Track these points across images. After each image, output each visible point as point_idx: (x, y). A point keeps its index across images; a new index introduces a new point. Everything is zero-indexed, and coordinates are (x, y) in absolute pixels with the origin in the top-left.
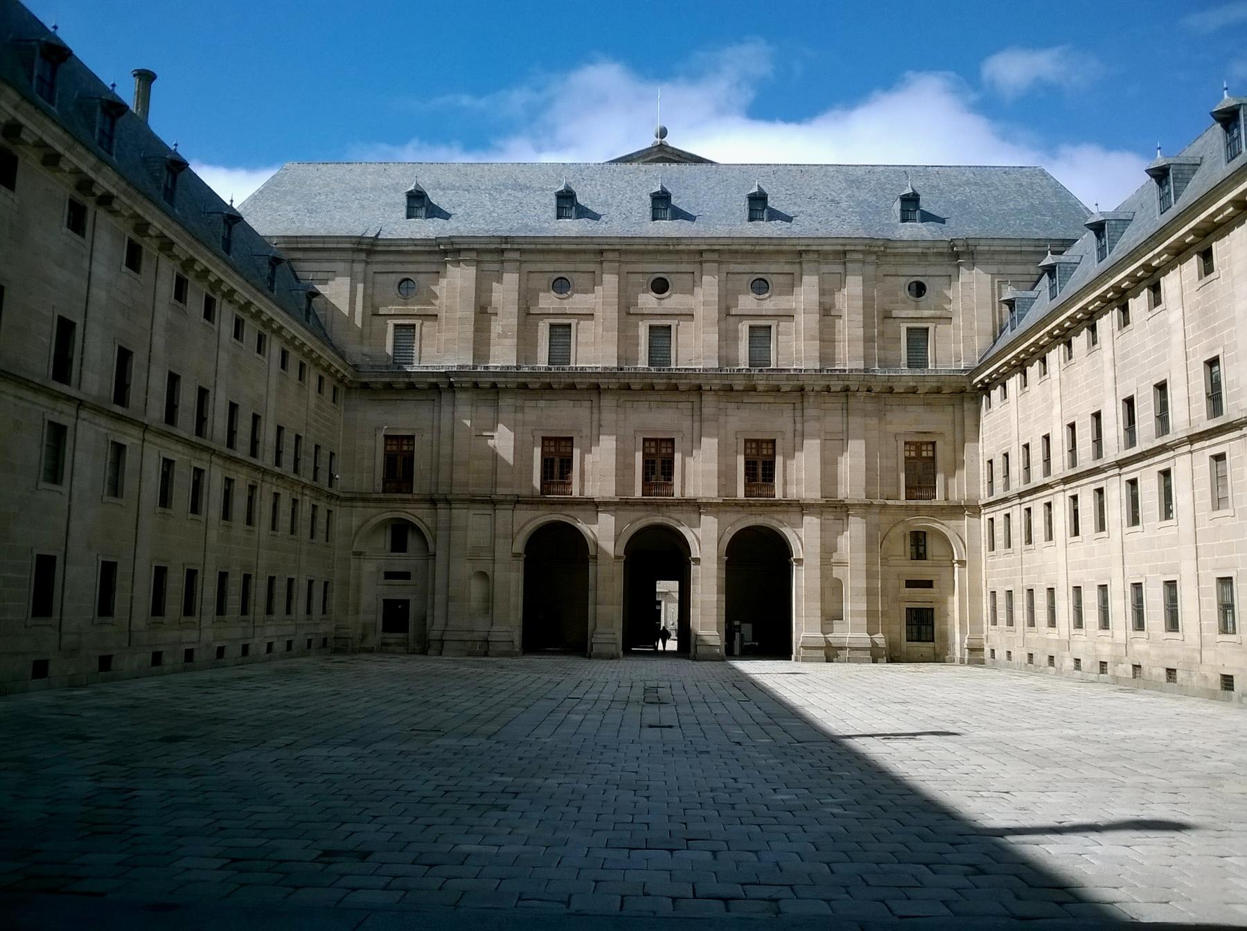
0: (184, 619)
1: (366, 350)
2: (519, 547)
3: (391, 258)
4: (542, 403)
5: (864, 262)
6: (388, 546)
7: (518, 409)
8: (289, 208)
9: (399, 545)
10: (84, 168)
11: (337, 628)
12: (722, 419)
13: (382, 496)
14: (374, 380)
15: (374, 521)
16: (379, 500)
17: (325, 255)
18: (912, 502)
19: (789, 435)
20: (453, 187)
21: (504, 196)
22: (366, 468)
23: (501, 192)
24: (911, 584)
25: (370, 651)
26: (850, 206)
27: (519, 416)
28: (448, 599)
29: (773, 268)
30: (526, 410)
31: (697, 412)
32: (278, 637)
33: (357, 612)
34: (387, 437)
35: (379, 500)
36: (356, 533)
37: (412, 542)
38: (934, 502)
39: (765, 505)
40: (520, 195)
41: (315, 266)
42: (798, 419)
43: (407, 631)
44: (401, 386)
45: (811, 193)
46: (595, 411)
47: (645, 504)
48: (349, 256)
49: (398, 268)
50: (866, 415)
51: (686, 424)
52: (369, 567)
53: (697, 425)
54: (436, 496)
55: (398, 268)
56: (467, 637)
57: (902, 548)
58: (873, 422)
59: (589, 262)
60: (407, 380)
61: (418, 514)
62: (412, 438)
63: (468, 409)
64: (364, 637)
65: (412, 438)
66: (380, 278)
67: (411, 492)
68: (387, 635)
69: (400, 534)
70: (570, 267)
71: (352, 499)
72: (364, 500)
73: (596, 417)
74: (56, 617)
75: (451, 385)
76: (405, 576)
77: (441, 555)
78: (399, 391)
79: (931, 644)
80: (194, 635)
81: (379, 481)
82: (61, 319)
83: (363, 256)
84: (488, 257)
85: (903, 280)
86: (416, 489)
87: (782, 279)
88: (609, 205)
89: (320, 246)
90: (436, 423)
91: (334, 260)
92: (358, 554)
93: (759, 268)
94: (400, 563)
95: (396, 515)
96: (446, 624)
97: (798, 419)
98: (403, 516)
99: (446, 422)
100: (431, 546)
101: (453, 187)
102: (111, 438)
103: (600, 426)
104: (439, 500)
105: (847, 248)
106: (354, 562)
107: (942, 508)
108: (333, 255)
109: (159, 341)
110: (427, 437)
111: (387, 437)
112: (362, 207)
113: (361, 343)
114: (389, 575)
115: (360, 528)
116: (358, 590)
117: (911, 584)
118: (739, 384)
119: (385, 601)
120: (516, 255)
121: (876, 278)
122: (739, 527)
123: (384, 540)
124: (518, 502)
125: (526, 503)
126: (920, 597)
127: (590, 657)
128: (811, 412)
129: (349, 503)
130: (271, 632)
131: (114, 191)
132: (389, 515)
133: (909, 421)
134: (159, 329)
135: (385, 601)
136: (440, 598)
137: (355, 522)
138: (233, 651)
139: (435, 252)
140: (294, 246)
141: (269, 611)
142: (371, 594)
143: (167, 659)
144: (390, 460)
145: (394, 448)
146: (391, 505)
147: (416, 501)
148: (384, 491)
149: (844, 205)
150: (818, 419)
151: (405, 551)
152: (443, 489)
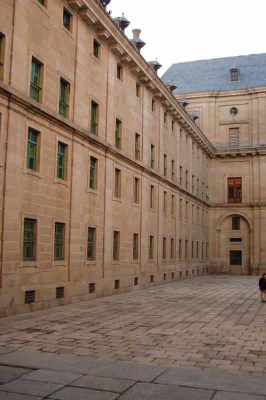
0: (171, 260)
1: (217, 140)
3: (226, 99)
6: (231, 227)
8: (178, 82)
9: (236, 226)
10: (144, 70)
11: (211, 263)
13: (228, 205)
14: (222, 153)
15: (225, 216)
16: (226, 207)
17: (197, 100)
20: (248, 66)
22: (219, 193)
25: (225, 273)
32: (196, 267)
33: (219, 257)
34: (229, 178)
35: (228, 207)
36: (217, 222)
37: (242, 224)
41: (193, 106)
43: (241, 264)
44: (245, 155)
48: (208, 99)
49: (230, 103)
52: (223, 236)
54: (253, 204)
55: (230, 103)
60: (237, 153)
62: (241, 178)
64: (222, 267)
65: (241, 178)
66: (221, 108)
67: (241, 203)
68: (232, 266)
69: (236, 221)
71: (216, 207)
72: (220, 207)
74: (139, 260)
75: (258, 154)
76: (240, 240)
78: (244, 157)
80: (173, 267)
81: (226, 198)
82: (136, 133)
83: (214, 99)
89: (195, 97)
90: (251, 171)
91: (201, 102)
92: (219, 231)
94: (236, 234)
95: (235, 213)
96: (260, 262)
100: (251, 227)
101: (248, 66)
102: (151, 184)
104: (255, 206)
106: (217, 234)
108: (201, 100)
109: (161, 141)
110: (247, 178)
111: (229, 178)
112: (210, 78)
113: (215, 138)
114: (232, 240)
115: (218, 220)
116: (219, 247)
119: (231, 251)
123: (228, 223)
129: (214, 209)
130: (194, 265)
131: (151, 78)
134: (161, 137)
135: (231, 251)
137: (217, 216)
138: (184, 274)
139: (245, 95)
140: (173, 98)
141: (192, 257)
142: (225, 248)
143: (167, 276)
144: (230, 189)
145: (232, 183)
146: (233, 209)
147: (244, 206)
148: (228, 203)
151: (239, 229)
152: (256, 201)
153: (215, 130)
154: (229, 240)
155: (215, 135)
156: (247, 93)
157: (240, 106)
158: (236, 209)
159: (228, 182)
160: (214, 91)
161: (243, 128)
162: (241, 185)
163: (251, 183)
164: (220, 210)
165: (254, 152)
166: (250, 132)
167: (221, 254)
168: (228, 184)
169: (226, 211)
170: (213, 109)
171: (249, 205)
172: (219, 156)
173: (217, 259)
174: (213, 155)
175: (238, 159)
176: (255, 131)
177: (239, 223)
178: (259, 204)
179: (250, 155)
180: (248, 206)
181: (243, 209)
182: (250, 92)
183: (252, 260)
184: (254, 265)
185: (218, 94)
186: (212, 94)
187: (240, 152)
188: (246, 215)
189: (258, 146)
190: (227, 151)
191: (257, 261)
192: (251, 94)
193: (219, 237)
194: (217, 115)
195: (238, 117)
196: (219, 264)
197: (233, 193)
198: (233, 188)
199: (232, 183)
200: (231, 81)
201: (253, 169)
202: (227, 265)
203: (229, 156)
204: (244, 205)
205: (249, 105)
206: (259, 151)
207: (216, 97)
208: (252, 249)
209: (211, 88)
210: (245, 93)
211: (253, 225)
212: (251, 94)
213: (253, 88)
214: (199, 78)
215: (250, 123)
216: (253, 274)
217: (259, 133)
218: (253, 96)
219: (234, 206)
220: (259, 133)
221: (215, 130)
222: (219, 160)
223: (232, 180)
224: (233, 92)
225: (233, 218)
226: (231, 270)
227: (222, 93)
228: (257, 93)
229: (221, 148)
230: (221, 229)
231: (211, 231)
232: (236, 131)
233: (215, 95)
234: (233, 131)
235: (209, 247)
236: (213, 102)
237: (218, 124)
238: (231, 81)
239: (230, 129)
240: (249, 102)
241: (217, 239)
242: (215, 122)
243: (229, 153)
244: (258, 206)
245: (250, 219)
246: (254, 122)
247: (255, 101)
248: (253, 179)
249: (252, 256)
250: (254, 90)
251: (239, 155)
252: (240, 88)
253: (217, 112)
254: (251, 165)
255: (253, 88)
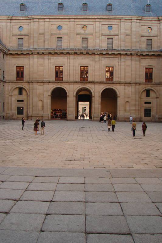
1: (11, 45)
2: (50, 94)
4: (55, 58)
5: (136, 22)
6: (18, 94)
7: (49, 59)
9: (20, 93)
11: (7, 114)
12: (100, 61)
13: (16, 81)
14: (13, 52)
16: (15, 82)
18: (147, 83)
19: (117, 66)
21: (45, 5)
22: (11, 75)
23: (44, 3)
24: (146, 103)
25: (14, 119)
26: (133, 8)
27: (49, 61)
28: (33, 107)
29: (113, 23)
30: (51, 59)
31: (94, 59)
33: (11, 110)
34: (17, 67)
35: (15, 82)
37: (24, 92)
38: (152, 83)
39: (60, 83)
40: (49, 4)
42: (120, 62)
45: (123, 4)
46: (69, 60)
47: (81, 83)
49: (18, 24)
50: (136, 61)
51: (91, 63)
53: (94, 63)
55: (18, 24)
56: (38, 115)
57: (144, 94)
58: (138, 63)
59: (67, 22)
60: (21, 52)
61: (24, 85)
62: (23, 67)
63: (37, 59)
64: (13, 116)
65: (23, 67)
67: (23, 80)
69: (21, 90)
70: (62, 23)
71: (9, 82)
72: (12, 82)
73: (69, 61)
75: (32, 53)
76: (22, 101)
77: (31, 96)
78: (19, 55)
79: (150, 117)
83: (9, 21)
84: (41, 20)
85: (146, 27)
86: (24, 80)
87: (116, 26)
88: (72, 7)
90: (29, 63)
92: (11, 96)
93: (110, 23)
94: (21, 98)
96: (33, 113)
97: (120, 62)
98: (21, 86)
99: (31, 63)
100: (28, 94)
101: (32, 3)
103: (70, 63)
105: (132, 18)
106: (10, 98)
107: (154, 84)
111: (17, 67)
112: (9, 8)
114: (18, 101)
117: (146, 103)
118: (104, 52)
120: (48, 20)
121: (139, 26)
122: (104, 88)
123: (17, 92)
124: (49, 82)
125: (51, 83)
126: (148, 106)
127: (67, 120)
128: (123, 60)
132: (18, 86)
133: (147, 62)
136: (31, 106)
137: (10, 88)
142: (15, 105)
144: (18, 73)
145: (19, 69)
148: (16, 80)
149: (132, 7)
150: (124, 62)
152: (31, 80)
153: (10, 39)
154: (17, 101)
155: (10, 42)
156: (28, 19)
157: (24, 26)
158: (20, 84)
159: (17, 69)
160: (9, 16)
161: (26, 38)
162: (23, 70)
163: (29, 70)
164: (12, 84)
165: (30, 52)
166: (29, 41)
167: (12, 108)
168: (17, 70)
169: (15, 85)
170: (9, 26)
171: (27, 82)
172: (11, 54)
173: (10, 112)
174: (7, 53)
175: (22, 56)
176: (32, 41)
177: (22, 92)
178: (33, 81)
179: (28, 54)
180: (26, 82)
181: (24, 84)
182: (30, 18)
183: (28, 112)
184: (30, 115)
185: (12, 18)
186: (8, 17)
187: (23, 52)
188: (26, 87)
189: (33, 49)
190: (15, 51)
191: (31, 112)
192: (30, 19)
193: (11, 99)
194: (11, 30)
195: (23, 32)
196: (11, 114)
197: (19, 75)
198: (19, 72)
199: (19, 69)
200: (21, 11)
201: (30, 62)
202: (15, 115)
203: (17, 54)
204: (24, 82)
205: (30, 25)
206: (33, 52)
207: (11, 20)
208: (28, 106)
209: (8, 14)
210: (27, 19)
211: (29, 93)
212: (30, 19)
213: (31, 16)
214: (3, 7)
215: (30, 36)
216: (29, 119)
217: (33, 42)
218: (32, 21)
219: (19, 82)
220: (33, 42)
221: (10, 39)
222: (11, 56)
223: (19, 68)
224: (20, 17)
225: (19, 89)
226: (18, 118)
227: (14, 17)
228: (34, 19)
229: (13, 49)
230: (12, 95)
231: (6, 96)
232: (22, 40)
233: (10, 18)
234: (20, 40)
235: (5, 105)
236: (9, 22)
237: (11, 35)
238: (21, 11)
239: (18, 39)
240: (29, 24)
241: (10, 101)
242: (10, 34)
243: (16, 52)
244: (32, 82)
245: (27, 89)
246: (31, 36)
247: (32, 24)
248: (30, 67)
249: (28, 110)
250: (32, 17)
251: (22, 54)
252: (25, 15)
253: (11, 28)
254: (29, 60)
255: (31, 16)
